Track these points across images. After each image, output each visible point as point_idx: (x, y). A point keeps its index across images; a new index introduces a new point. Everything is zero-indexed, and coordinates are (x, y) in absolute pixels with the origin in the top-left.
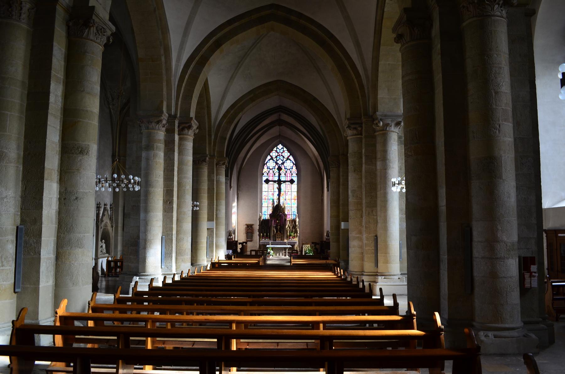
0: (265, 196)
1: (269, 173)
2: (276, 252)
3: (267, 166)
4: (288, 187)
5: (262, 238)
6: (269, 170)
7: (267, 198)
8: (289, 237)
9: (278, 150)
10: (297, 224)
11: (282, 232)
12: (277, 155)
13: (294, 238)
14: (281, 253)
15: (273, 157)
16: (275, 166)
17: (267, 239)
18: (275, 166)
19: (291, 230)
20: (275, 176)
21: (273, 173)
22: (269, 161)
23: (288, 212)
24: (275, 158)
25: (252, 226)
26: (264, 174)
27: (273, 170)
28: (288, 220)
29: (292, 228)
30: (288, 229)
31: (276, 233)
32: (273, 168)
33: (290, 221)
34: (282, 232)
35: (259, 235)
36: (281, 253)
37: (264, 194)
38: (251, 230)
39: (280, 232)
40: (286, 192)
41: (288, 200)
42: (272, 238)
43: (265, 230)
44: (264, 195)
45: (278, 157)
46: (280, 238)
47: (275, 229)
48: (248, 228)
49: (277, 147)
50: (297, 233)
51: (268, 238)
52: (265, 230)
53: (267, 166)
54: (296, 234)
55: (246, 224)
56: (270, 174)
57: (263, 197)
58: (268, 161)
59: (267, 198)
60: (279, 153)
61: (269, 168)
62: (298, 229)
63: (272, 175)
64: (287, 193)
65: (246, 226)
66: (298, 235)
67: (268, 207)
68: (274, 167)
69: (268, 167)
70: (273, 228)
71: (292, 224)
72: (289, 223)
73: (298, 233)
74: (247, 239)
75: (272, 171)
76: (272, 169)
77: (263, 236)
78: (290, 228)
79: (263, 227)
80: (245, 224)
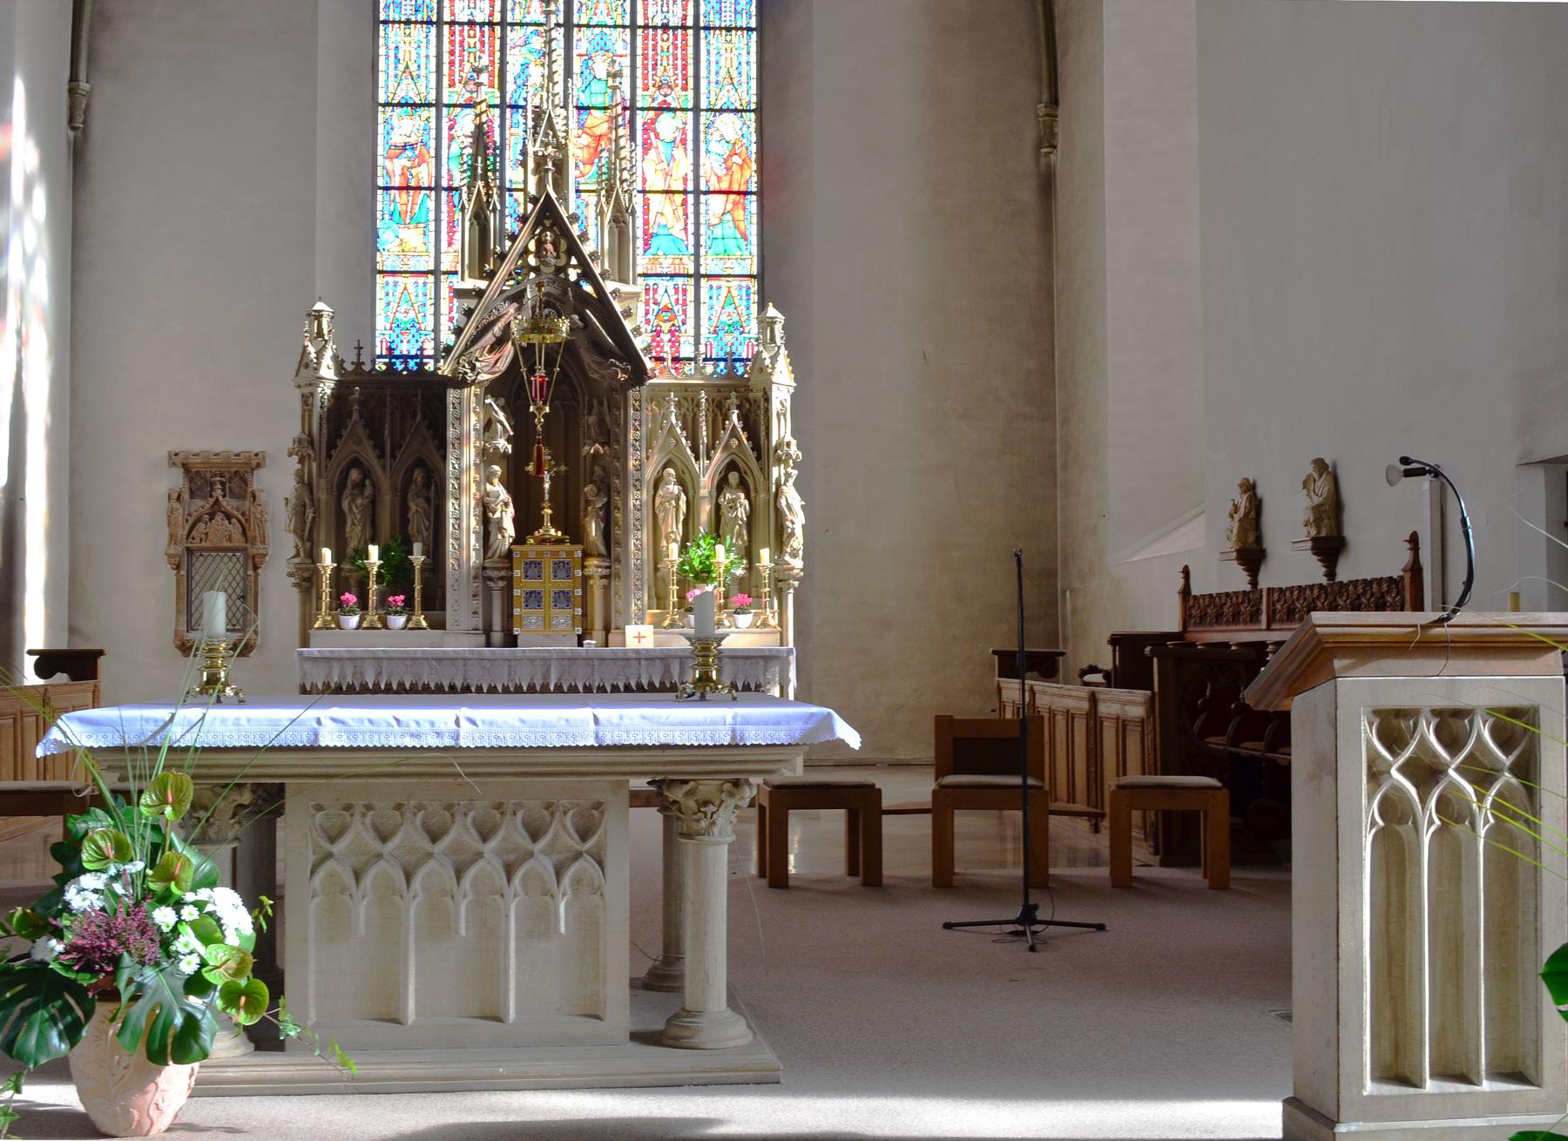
0: (398, 165)
2: (362, 910)
4: (665, 61)
5: (338, 606)
7: (424, 175)
8: (684, 585)
10: (781, 430)
11: (593, 529)
13: (740, 610)
14: (538, 924)
17: (399, 621)
19: (705, 511)
23: (666, 327)
25: (245, 482)
28: (661, 393)
29: (721, 485)
30: (675, 489)
31: (519, 540)
33: (687, 395)
34: (593, 529)
35: (307, 581)
36: (538, 924)
37: (399, 128)
38: (235, 530)
39: (574, 532)
40: (641, 118)
41: (656, 201)
42: (460, 606)
43: (373, 502)
44: (399, 140)
46: (563, 598)
47: (499, 490)
48: (200, 505)
50: (780, 537)
51: (408, 606)
52: (373, 502)
54: (765, 555)
55: (173, 459)
57: (391, 169)
59: (424, 175)
62: (792, 497)
64: (649, 127)
65: (177, 480)
66: (798, 563)
67: (436, 272)
70: (471, 477)
71: (714, 436)
72: (683, 418)
73: (798, 542)
74: (190, 628)
77: (349, 581)
78: (687, 483)
79: (354, 475)
80: (163, 452)
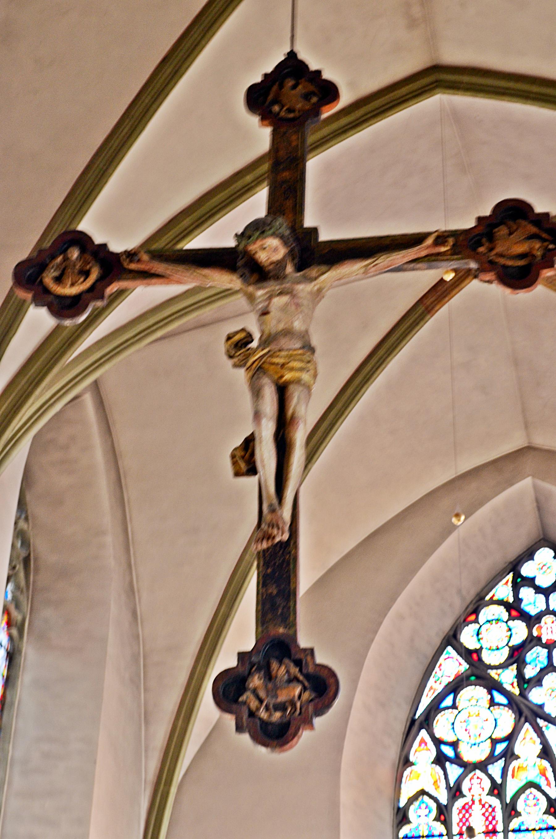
1: (459, 803)
3: (438, 742)
6: (454, 771)
9: (526, 593)
12: (517, 640)
15: (488, 658)
16: (511, 738)
18: (511, 738)
20: (514, 824)
21: (495, 802)
22: (448, 701)
24: (504, 666)
26: (412, 814)
27: (495, 770)
32: (492, 759)
45: (529, 657)
49: (517, 575)
53: (438, 742)
56: (467, 808)
58: (441, 697)
60: (539, 618)
61: (458, 760)
63: (489, 817)
68: (500, 748)
69: (448, 751)
75: (487, 784)
76: (482, 766)
